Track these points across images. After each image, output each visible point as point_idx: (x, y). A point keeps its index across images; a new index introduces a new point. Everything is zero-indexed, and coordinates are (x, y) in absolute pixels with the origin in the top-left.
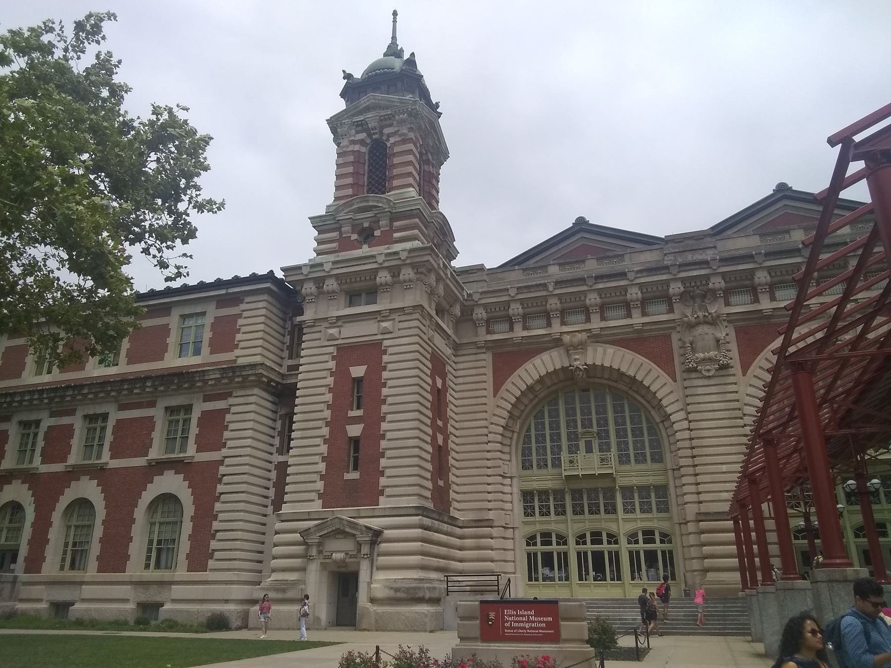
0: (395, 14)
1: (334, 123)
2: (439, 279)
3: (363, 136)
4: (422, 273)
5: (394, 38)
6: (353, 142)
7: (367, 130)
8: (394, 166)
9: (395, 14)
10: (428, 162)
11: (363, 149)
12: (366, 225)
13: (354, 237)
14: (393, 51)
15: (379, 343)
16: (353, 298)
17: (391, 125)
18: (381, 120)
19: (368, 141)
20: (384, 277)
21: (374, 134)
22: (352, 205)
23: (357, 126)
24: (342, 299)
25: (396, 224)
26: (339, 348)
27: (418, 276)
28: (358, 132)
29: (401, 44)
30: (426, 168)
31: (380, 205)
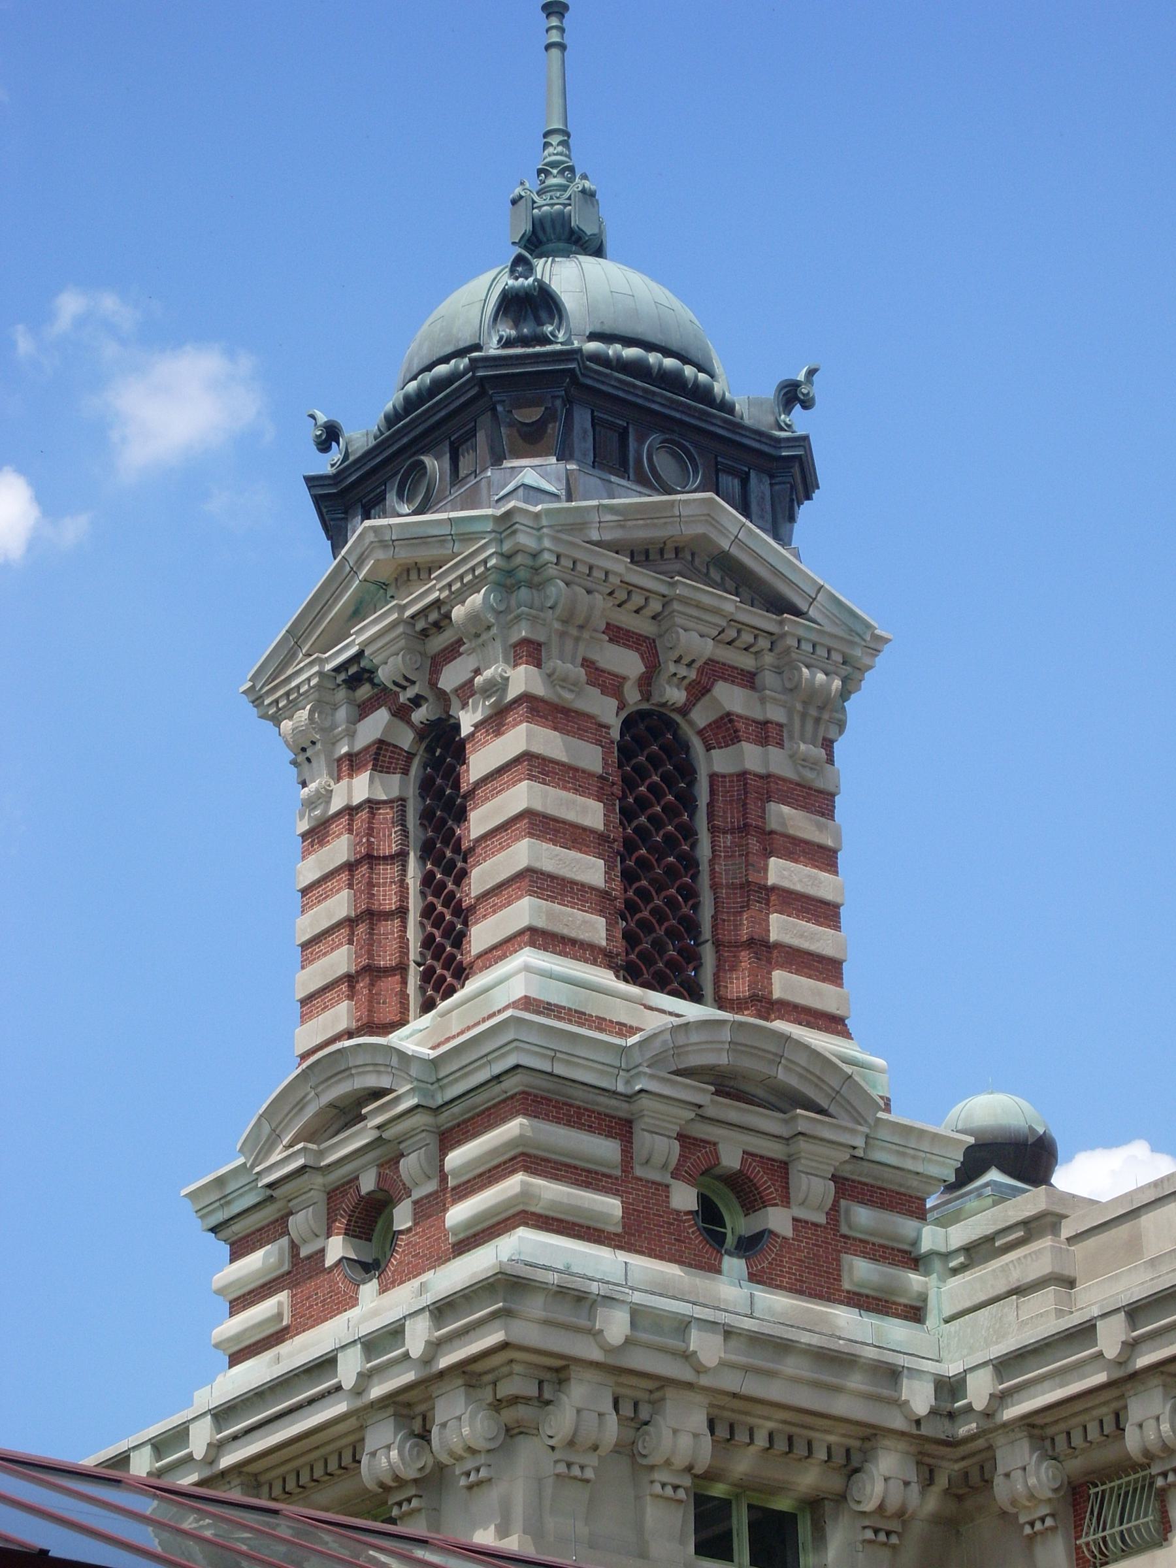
3: (377, 724)
4: (515, 1400)
7: (383, 696)
10: (726, 730)
11: (389, 787)
12: (368, 1183)
17: (452, 652)
18: (425, 633)
19: (406, 739)
21: (417, 701)
22: (301, 1105)
23: (353, 682)
25: (456, 1158)
27: (510, 1415)
28: (364, 710)
30: (721, 761)
31: (384, 1082)
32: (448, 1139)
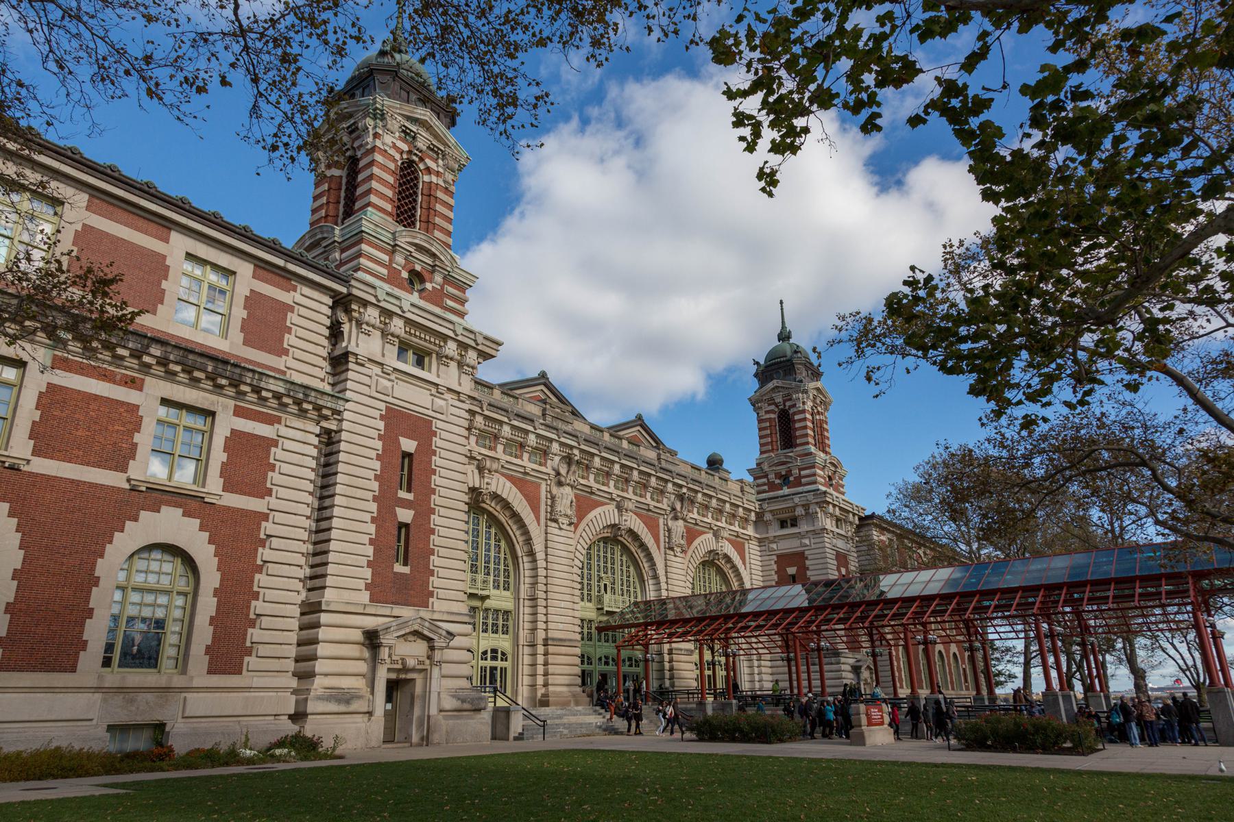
0: (781, 302)
1: (754, 403)
2: (834, 506)
5: (783, 322)
6: (767, 412)
8: (796, 429)
9: (781, 302)
11: (772, 416)
13: (777, 481)
14: (784, 336)
15: (803, 553)
16: (783, 524)
20: (800, 511)
24: (776, 525)
25: (803, 473)
26: (778, 556)
29: (789, 327)
32: (800, 470)
